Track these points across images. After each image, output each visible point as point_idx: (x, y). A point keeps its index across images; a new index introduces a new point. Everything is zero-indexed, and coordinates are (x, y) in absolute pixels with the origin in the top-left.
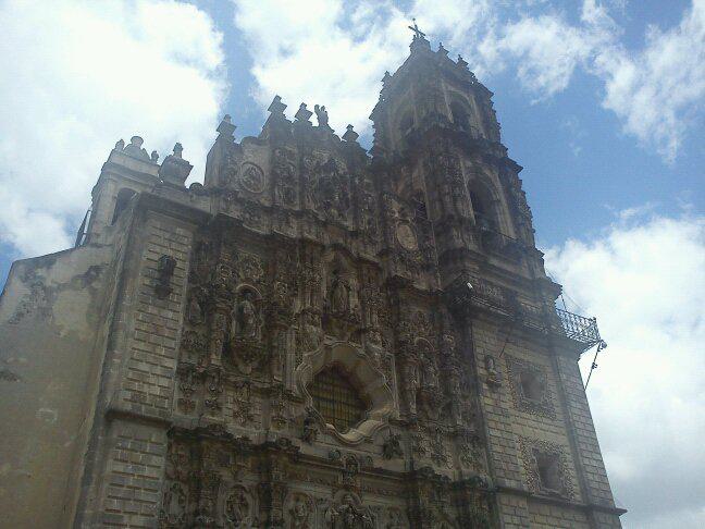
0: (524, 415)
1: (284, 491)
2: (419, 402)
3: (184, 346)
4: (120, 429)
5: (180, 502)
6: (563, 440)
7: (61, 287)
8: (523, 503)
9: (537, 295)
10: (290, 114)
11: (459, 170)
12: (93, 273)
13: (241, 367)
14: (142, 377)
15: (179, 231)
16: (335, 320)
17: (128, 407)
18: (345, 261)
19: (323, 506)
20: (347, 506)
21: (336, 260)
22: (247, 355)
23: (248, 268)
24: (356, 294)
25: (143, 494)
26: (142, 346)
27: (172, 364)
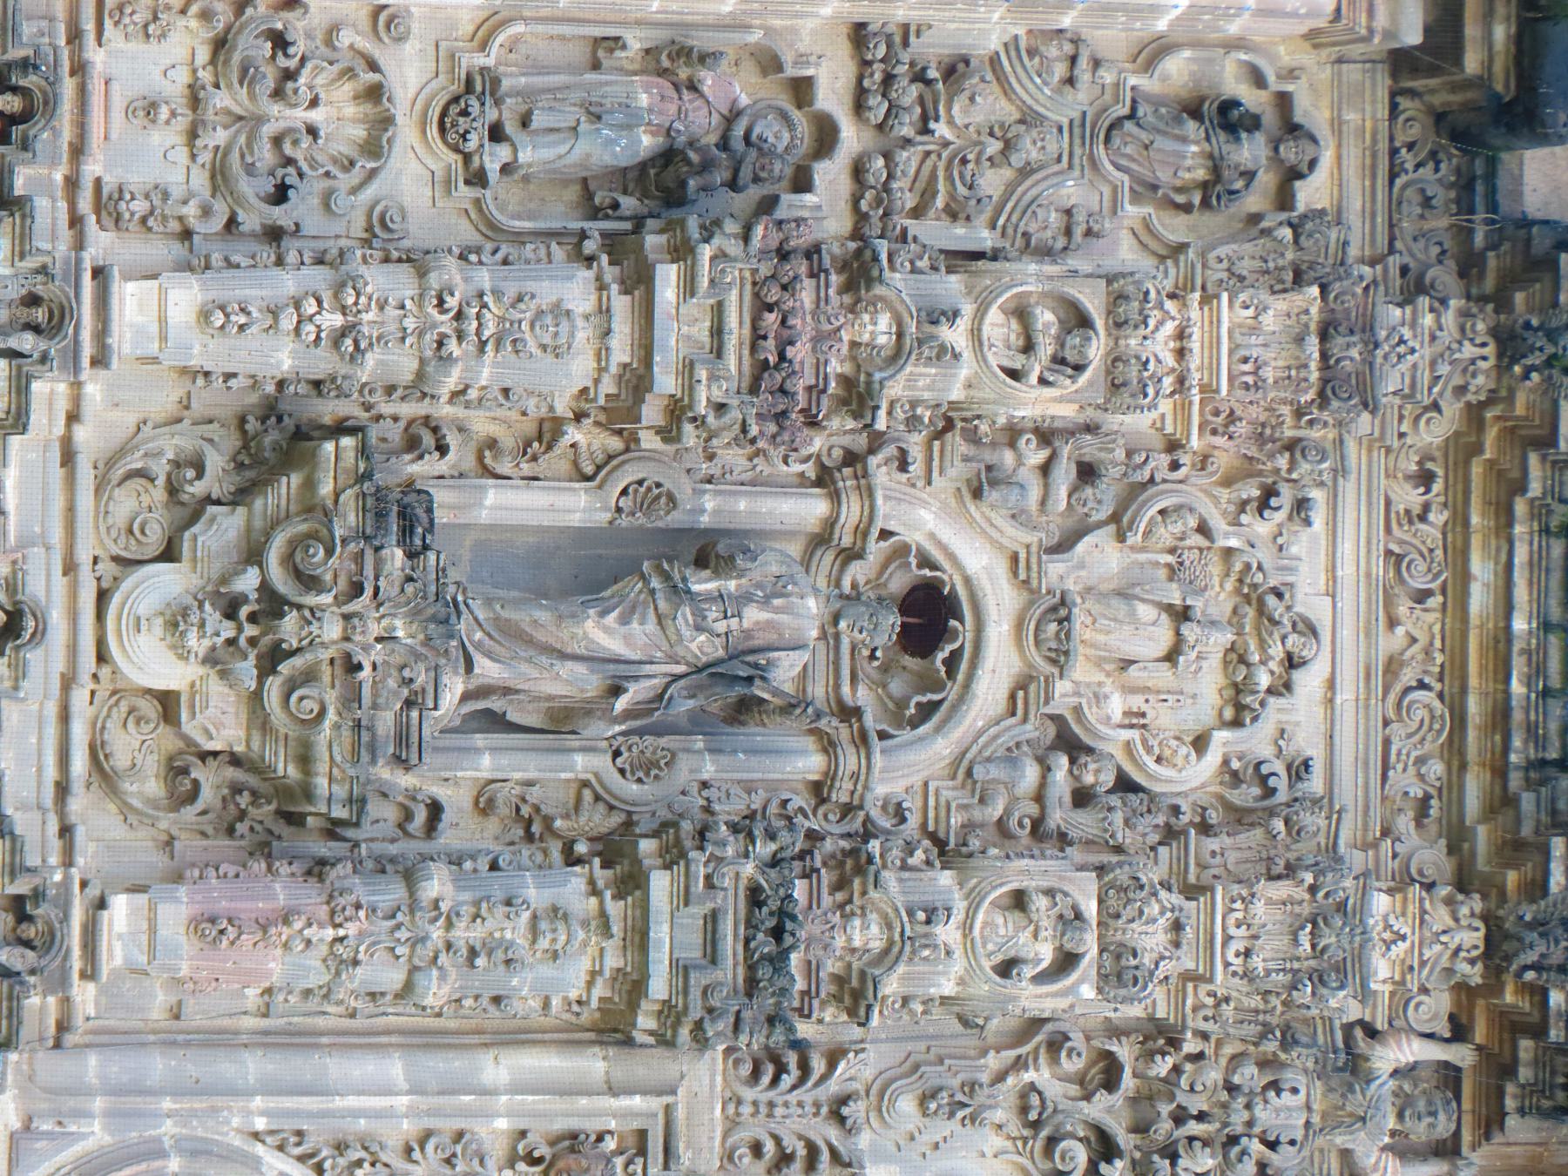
22: (273, 605)
23: (1182, 615)
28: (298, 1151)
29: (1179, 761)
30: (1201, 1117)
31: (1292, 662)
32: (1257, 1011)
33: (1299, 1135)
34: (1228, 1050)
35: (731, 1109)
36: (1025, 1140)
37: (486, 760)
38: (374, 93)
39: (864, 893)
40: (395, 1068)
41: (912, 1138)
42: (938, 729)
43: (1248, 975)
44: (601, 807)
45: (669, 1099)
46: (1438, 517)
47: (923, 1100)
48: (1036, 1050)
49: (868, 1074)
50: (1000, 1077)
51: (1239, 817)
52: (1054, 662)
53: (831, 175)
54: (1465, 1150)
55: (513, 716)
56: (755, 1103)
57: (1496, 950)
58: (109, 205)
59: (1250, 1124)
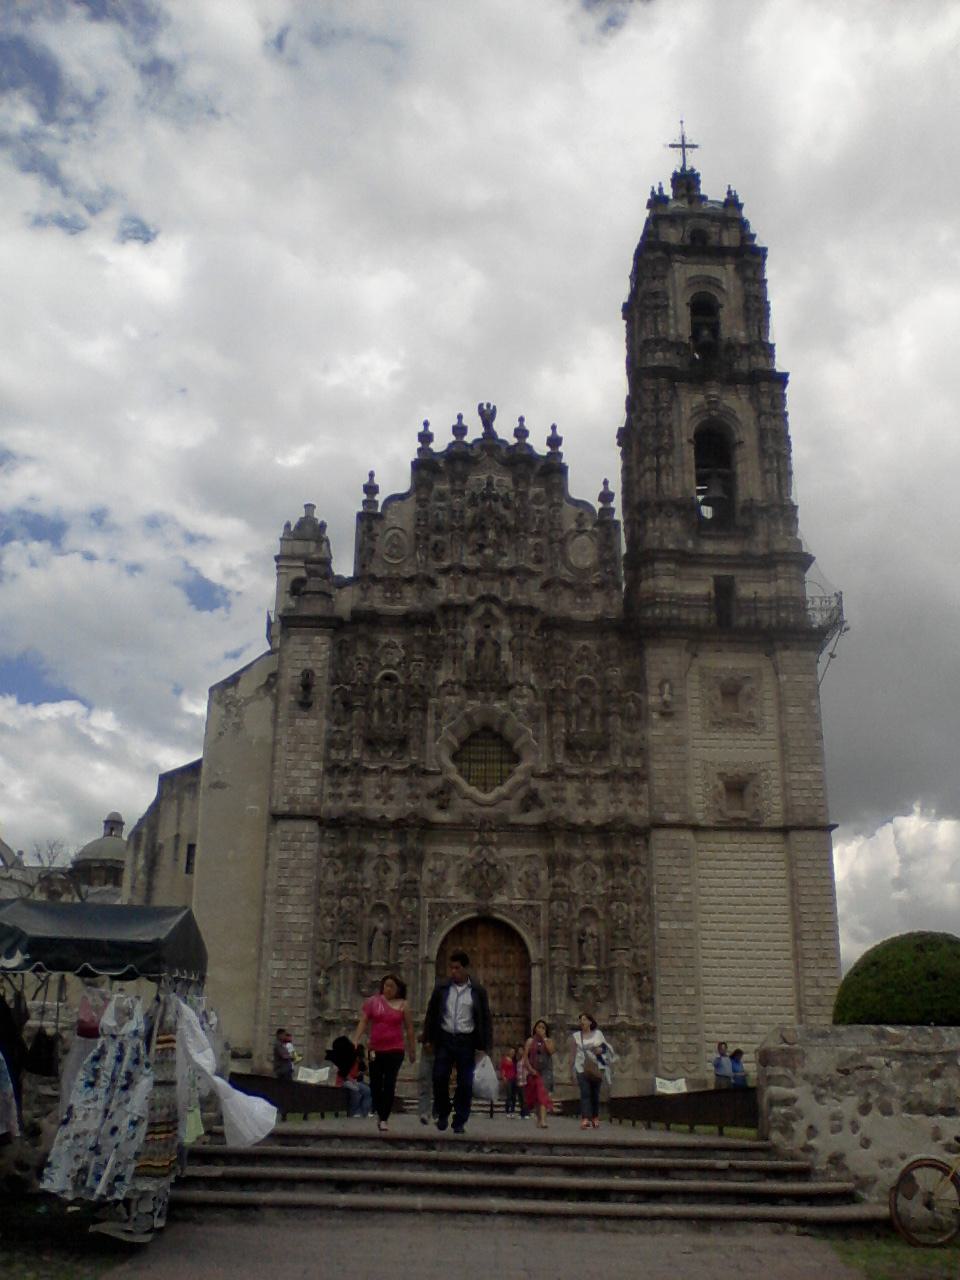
0: (712, 735)
1: (420, 859)
2: (570, 747)
3: (331, 744)
4: (284, 826)
5: (336, 873)
6: (774, 754)
7: (248, 701)
8: (688, 836)
9: (772, 572)
10: (441, 443)
11: (670, 426)
12: (272, 680)
13: (382, 753)
14: (295, 783)
15: (318, 639)
17: (287, 808)
18: (496, 611)
19: (459, 862)
20: (481, 860)
21: (488, 612)
24: (507, 647)
25: (302, 873)
26: (292, 756)
27: (318, 766)
38: (338, 731)
53: (346, 687)
57: (419, 623)
58: (346, 757)
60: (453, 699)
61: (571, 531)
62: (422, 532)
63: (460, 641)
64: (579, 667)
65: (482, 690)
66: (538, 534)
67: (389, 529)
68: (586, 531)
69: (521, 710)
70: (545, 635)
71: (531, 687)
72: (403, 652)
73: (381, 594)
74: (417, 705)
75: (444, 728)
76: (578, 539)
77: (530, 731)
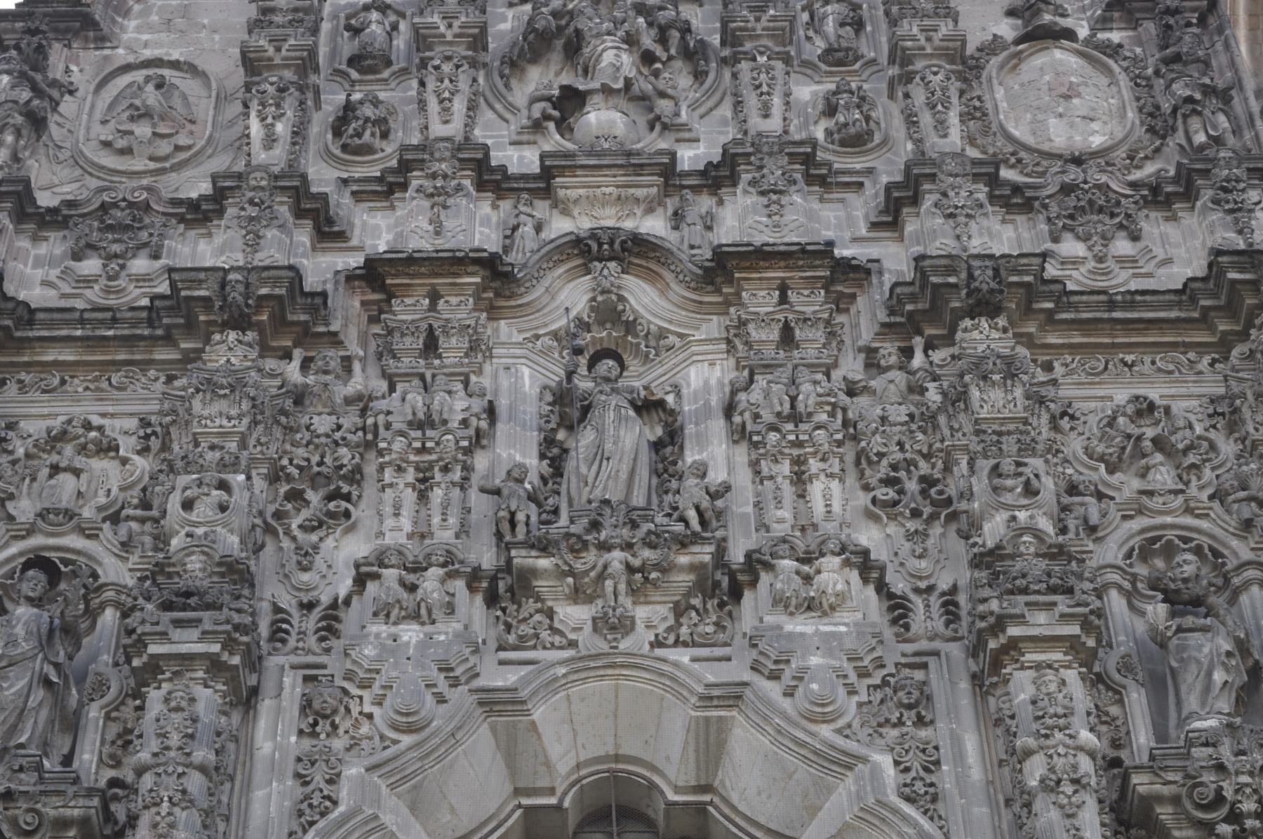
16: (544, 563)
23: (55, 469)
24: (718, 425)
28: (300, 834)
29: (132, 468)
30: (322, 457)
31: (88, 426)
32: (266, 428)
33: (334, 417)
34: (288, 447)
35: (300, 652)
36: (329, 527)
37: (86, 756)
39: (174, 565)
40: (259, 794)
41: (324, 576)
42: (100, 564)
43: (240, 417)
44: (122, 708)
45: (287, 667)
46: (23, 376)
47: (305, 569)
48: (281, 525)
49: (289, 597)
50: (294, 539)
51: (165, 447)
52: (71, 518)
54: (348, 353)
55: (65, 751)
56: (298, 641)
57: (240, 322)
59: (328, 436)
60: (411, 633)
61: (994, 46)
62: (277, 42)
63: (458, 406)
64: (1127, 484)
65: (578, 595)
66: (837, 57)
67: (127, 68)
68: (1070, 35)
69: (815, 660)
70: (918, 360)
71: (865, 564)
72: (142, 464)
73: (54, 274)
74: (188, 642)
75: (352, 771)
76: (1039, 60)
77: (885, 761)
